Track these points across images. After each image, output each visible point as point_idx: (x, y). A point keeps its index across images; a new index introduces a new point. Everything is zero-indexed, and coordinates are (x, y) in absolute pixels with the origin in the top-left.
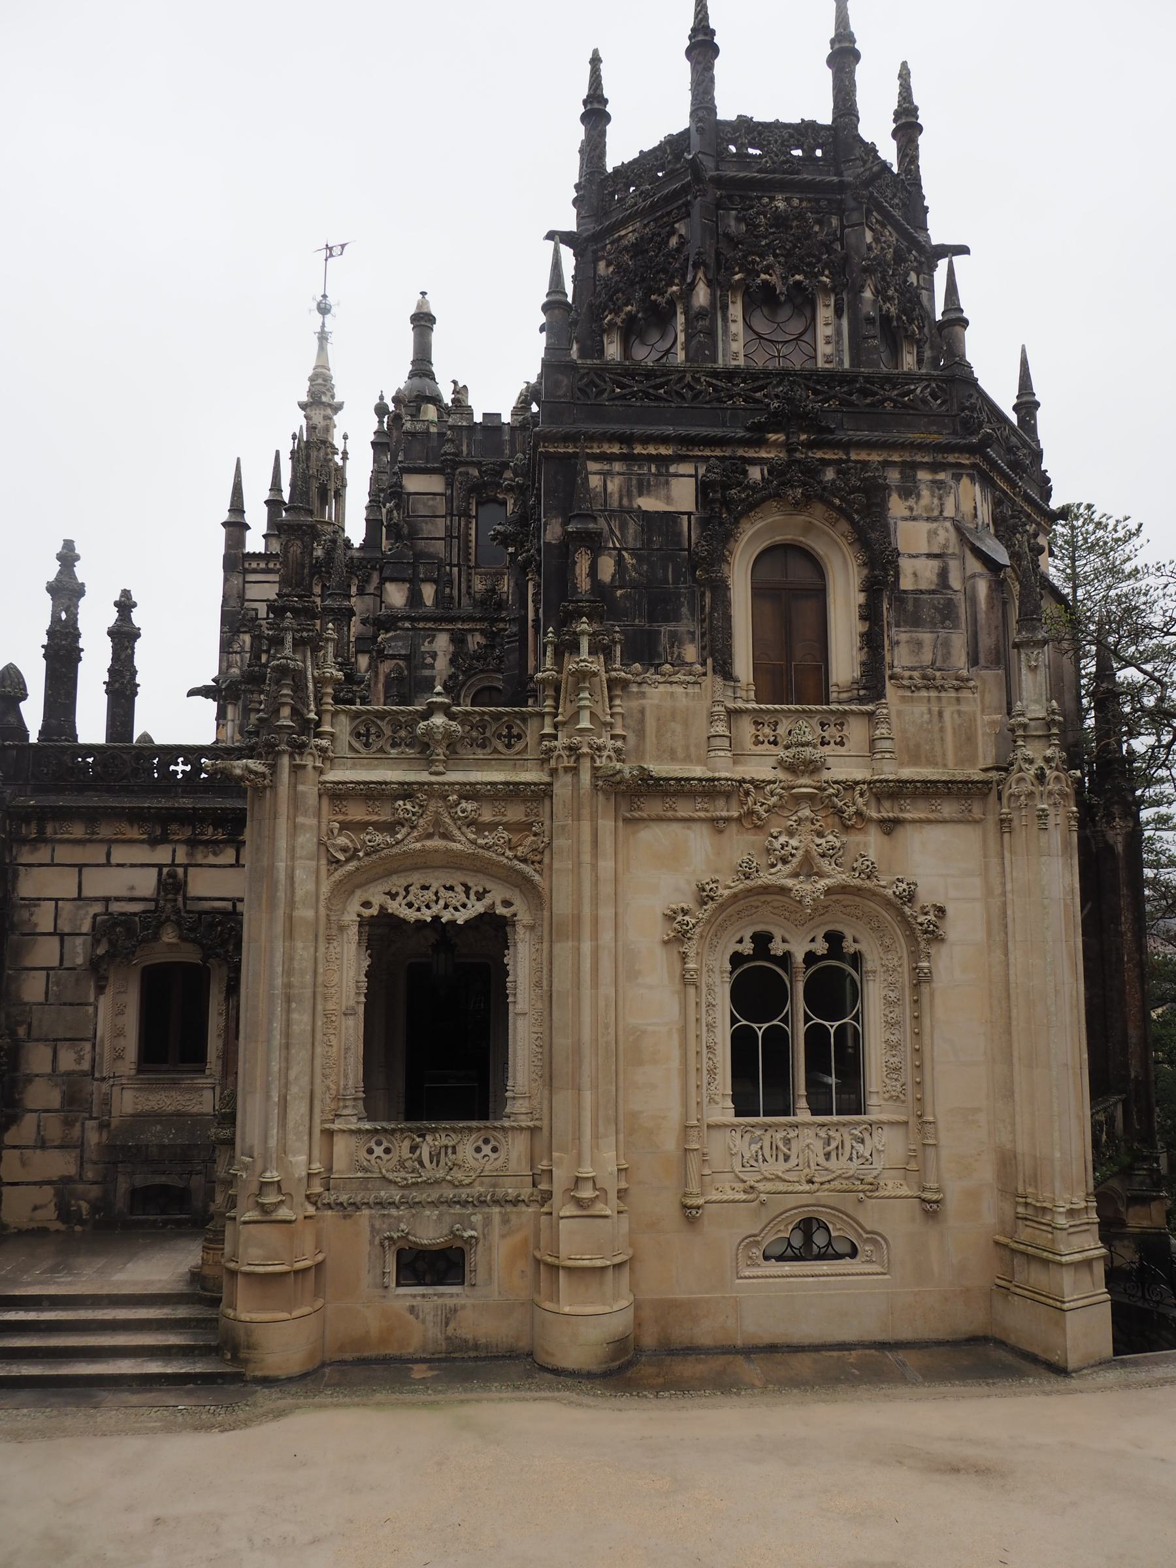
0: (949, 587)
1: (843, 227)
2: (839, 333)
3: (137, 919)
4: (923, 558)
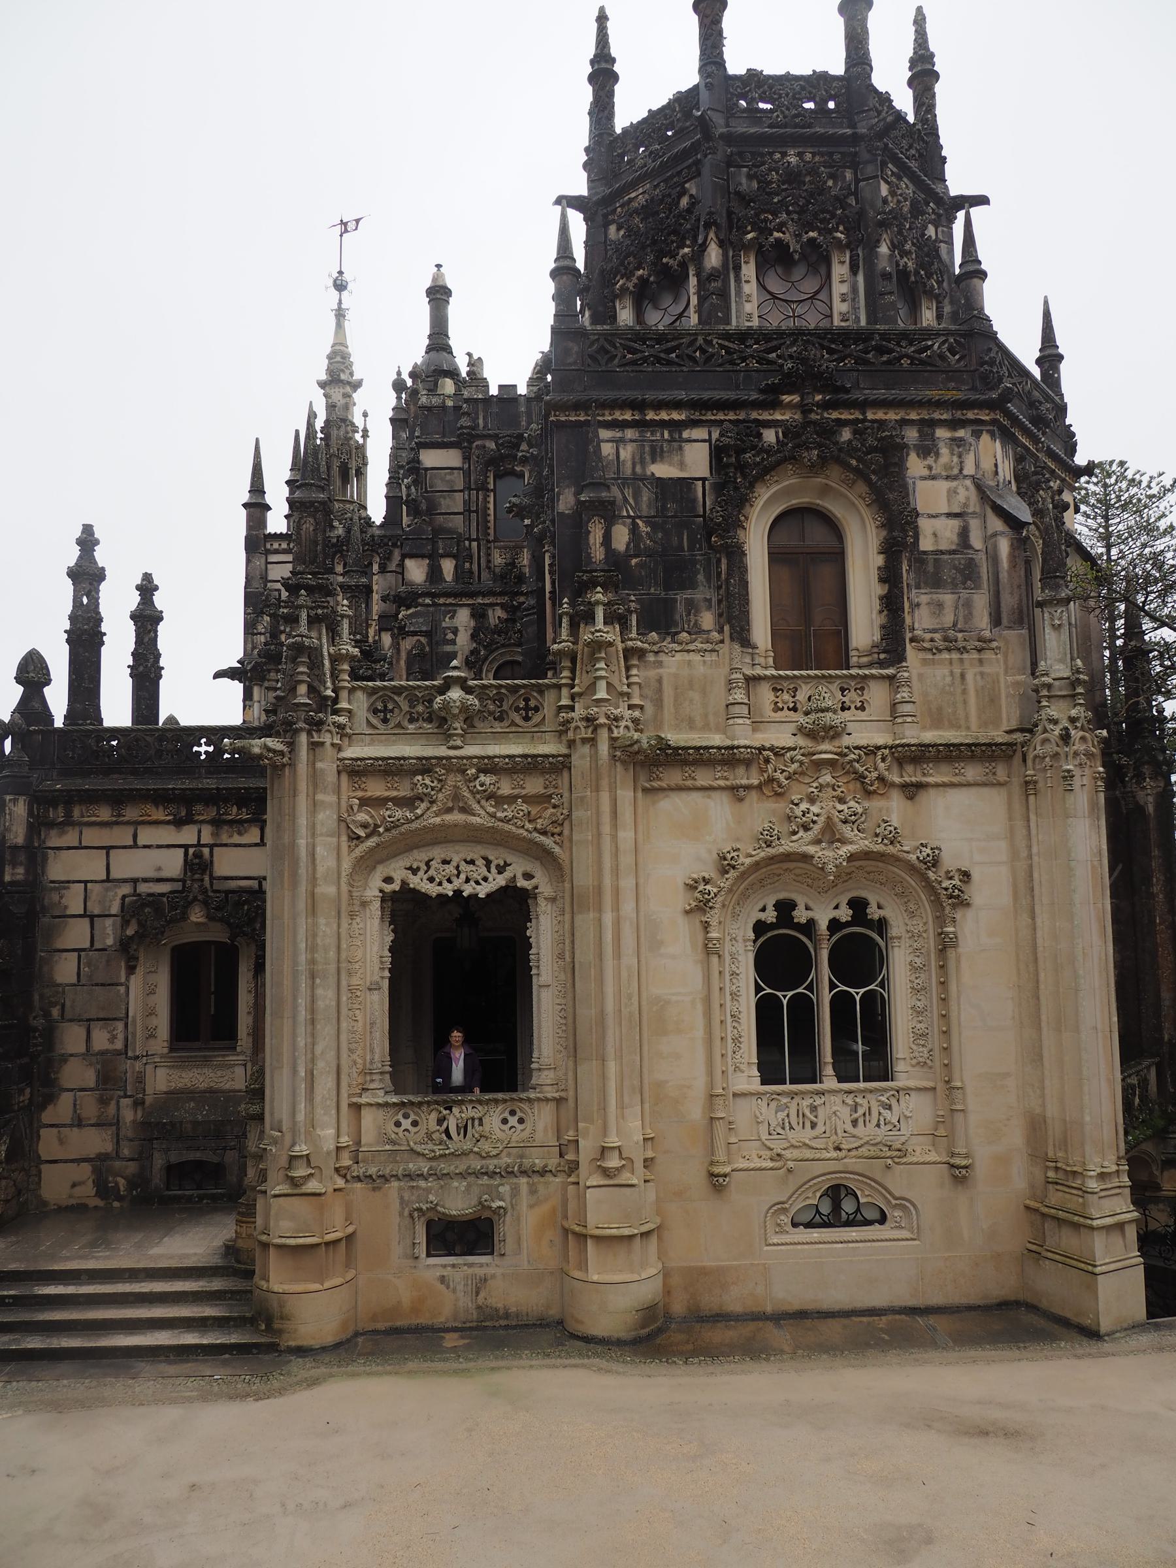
0: (970, 547)
1: (857, 181)
2: (854, 290)
3: (165, 899)
4: (943, 518)
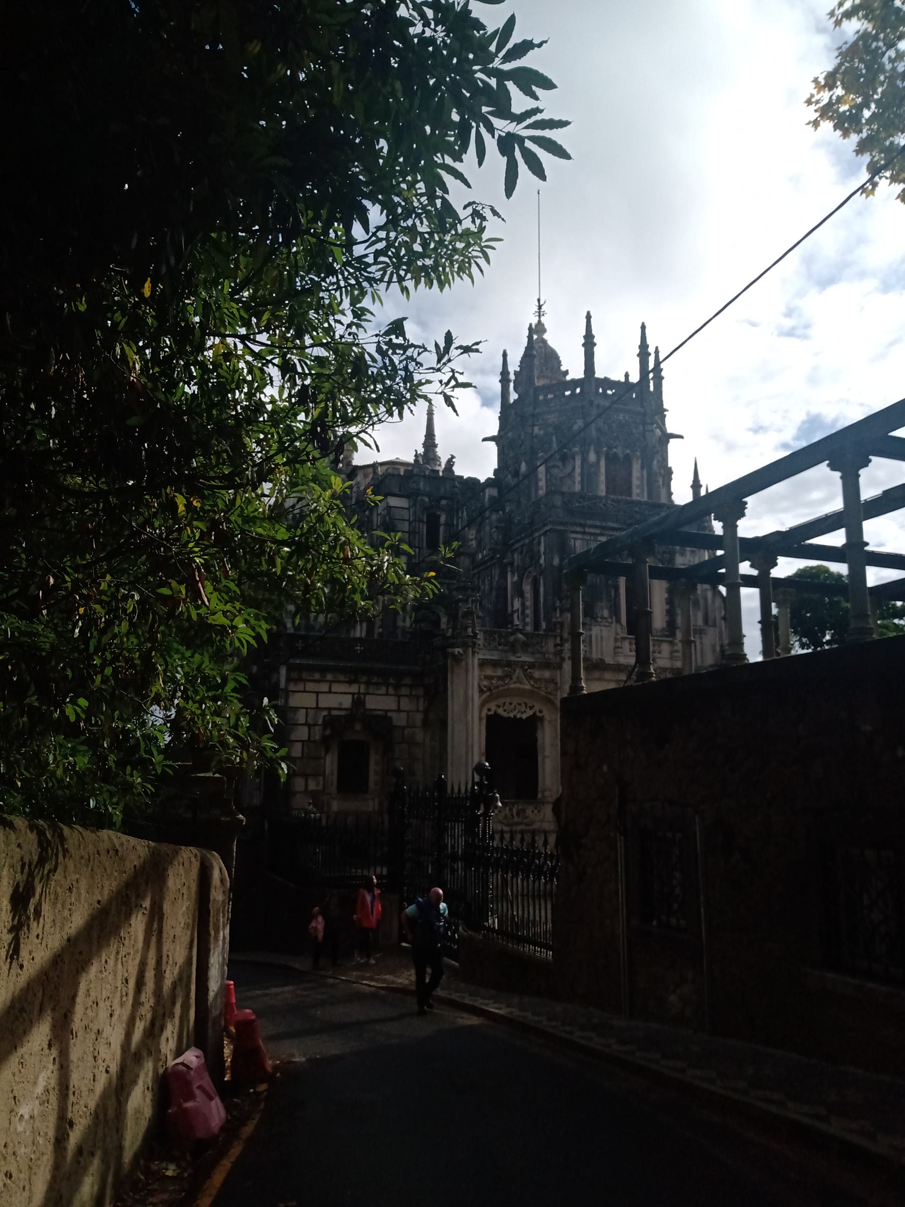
2: (642, 475)
